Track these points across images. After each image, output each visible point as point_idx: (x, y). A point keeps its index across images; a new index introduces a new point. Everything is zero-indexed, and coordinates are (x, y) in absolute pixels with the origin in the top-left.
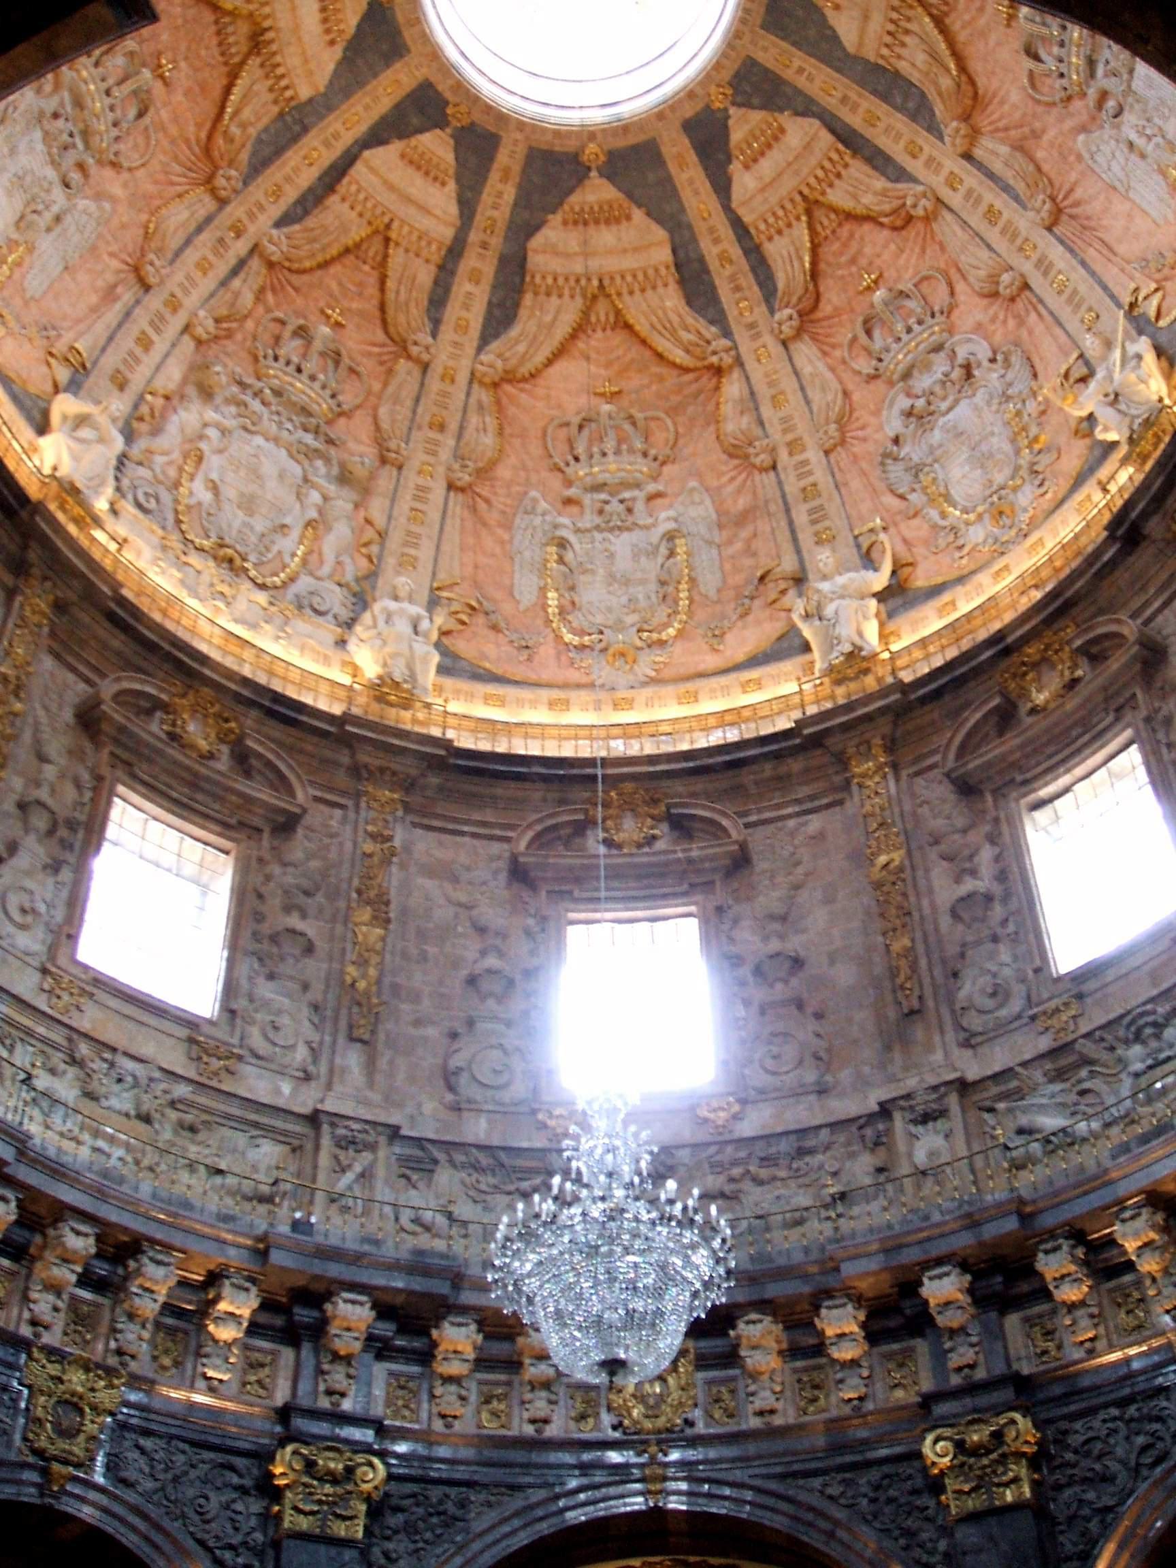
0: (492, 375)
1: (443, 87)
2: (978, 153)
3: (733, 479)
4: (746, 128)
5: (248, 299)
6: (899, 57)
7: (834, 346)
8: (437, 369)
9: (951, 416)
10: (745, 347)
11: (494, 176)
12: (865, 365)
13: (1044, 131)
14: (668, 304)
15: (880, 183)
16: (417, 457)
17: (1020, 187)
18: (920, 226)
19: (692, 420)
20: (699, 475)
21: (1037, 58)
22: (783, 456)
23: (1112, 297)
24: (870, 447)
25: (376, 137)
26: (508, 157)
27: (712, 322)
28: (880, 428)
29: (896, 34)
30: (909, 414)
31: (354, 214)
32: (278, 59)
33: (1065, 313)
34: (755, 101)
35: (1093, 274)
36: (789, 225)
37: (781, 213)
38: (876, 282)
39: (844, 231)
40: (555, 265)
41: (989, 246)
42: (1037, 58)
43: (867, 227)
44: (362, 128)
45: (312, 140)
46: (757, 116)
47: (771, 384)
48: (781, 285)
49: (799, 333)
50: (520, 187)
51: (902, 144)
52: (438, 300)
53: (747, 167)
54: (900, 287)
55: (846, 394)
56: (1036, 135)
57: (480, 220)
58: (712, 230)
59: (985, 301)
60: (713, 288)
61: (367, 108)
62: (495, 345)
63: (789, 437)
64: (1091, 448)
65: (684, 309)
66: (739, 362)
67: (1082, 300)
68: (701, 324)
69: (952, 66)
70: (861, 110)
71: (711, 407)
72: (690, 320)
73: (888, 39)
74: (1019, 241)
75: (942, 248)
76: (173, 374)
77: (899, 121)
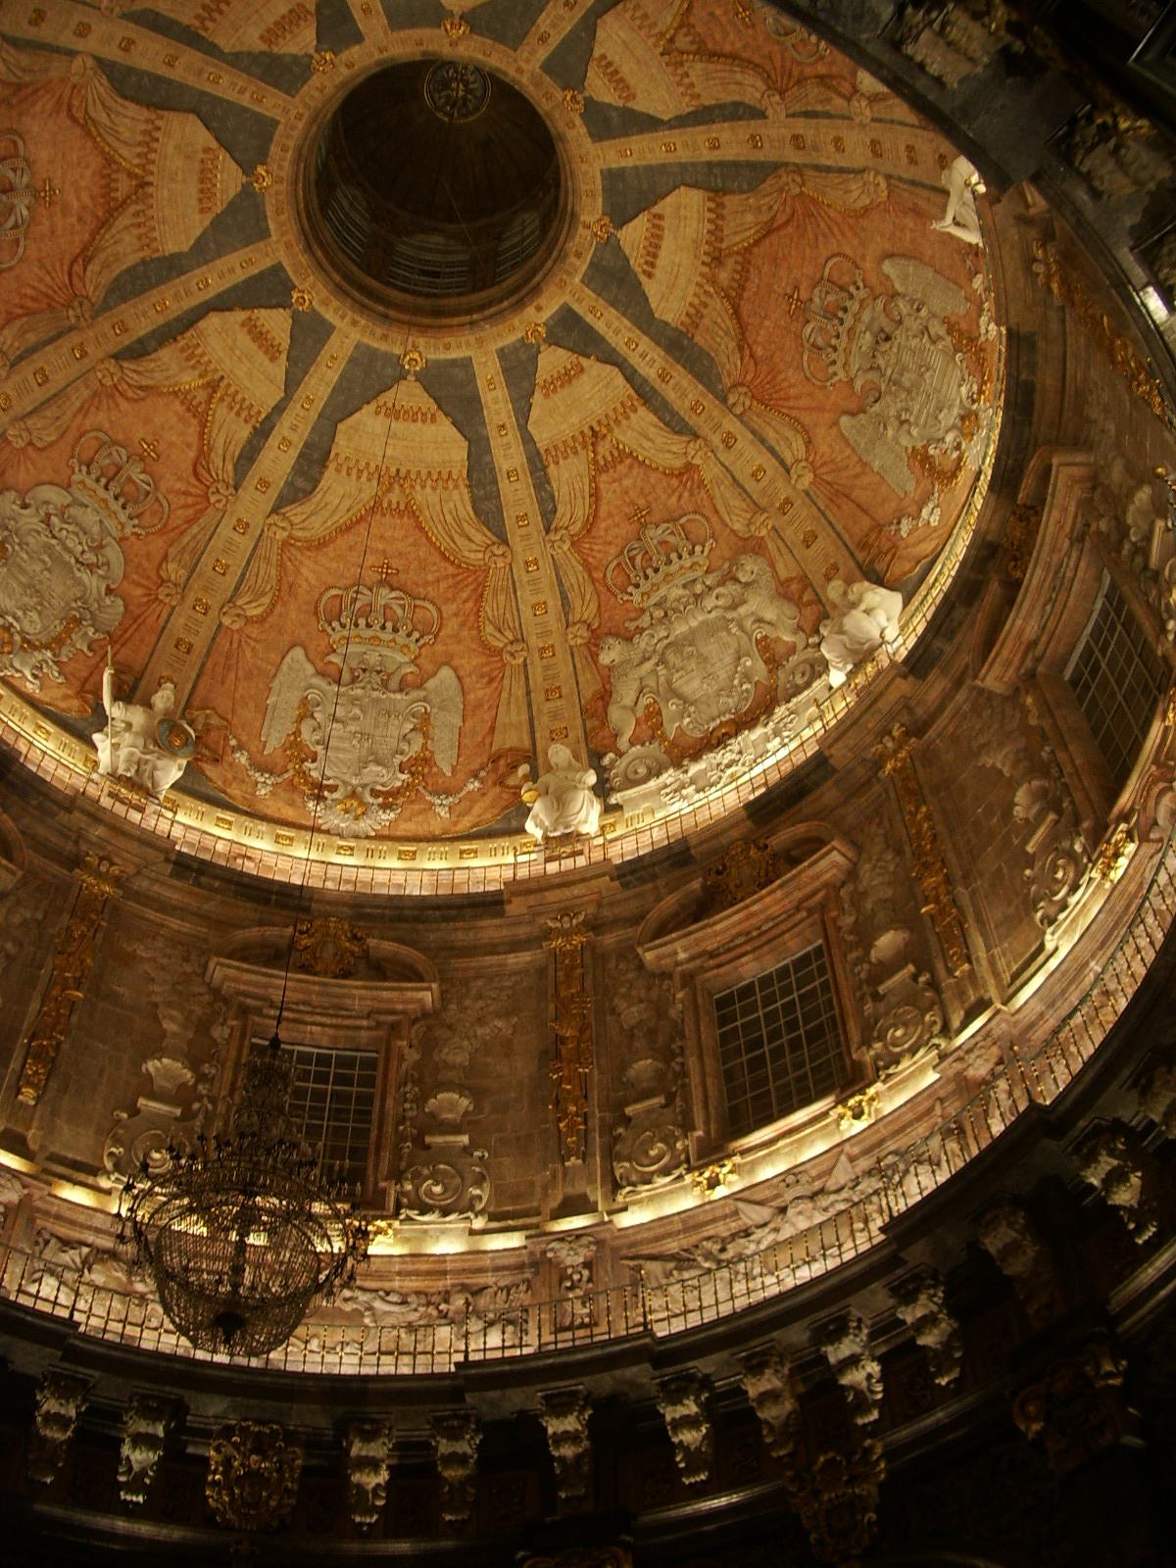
6: (147, 121)
11: (554, 41)
25: (651, 123)
29: (149, 141)
31: (693, 78)
32: (707, 237)
44: (660, 135)
45: (707, 155)
50: (533, 22)
61: (651, 151)
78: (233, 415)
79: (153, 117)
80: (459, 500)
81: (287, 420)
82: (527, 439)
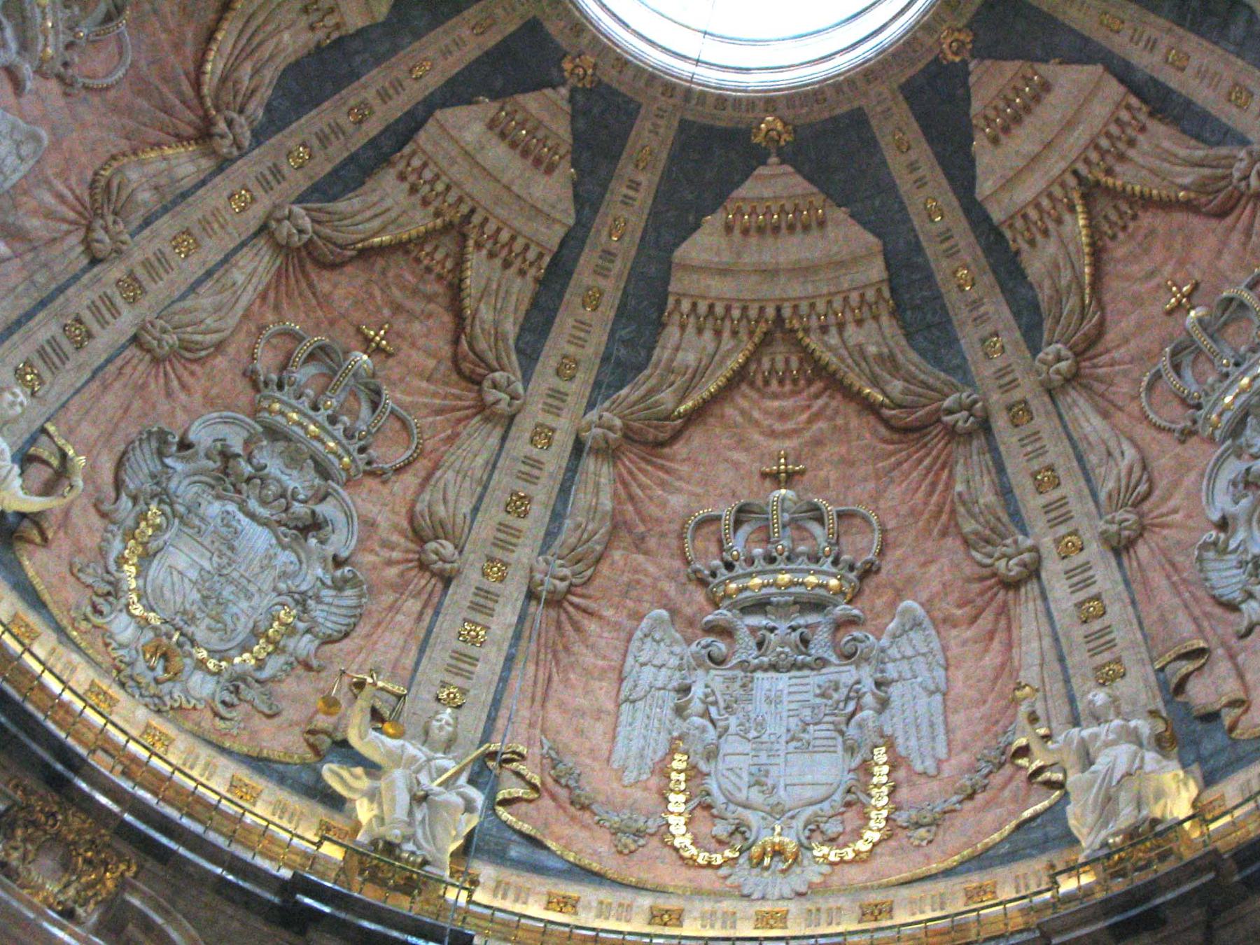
2: (590, 464)
3: (61, 198)
4: (546, 118)
6: (683, 327)
7: (277, 308)
9: (245, 520)
10: (246, 169)
12: (266, 363)
13: (646, 553)
14: (286, 36)
15: (510, 328)
17: (568, 535)
18: (470, 397)
19: (130, 111)
20: (56, 143)
21: (738, 523)
22: (115, 272)
23: (491, 719)
24: (164, 406)
27: (269, 109)
28: (194, 415)
30: (227, 456)
33: (439, 655)
34: (581, 124)
35: (504, 680)
36: (425, 202)
37: (440, 187)
38: (379, 349)
39: (433, 287)
41: (476, 510)
42: (738, 523)
43: (447, 318)
46: (562, 128)
47: (205, 224)
48: (341, 206)
49: (281, 248)
51: (571, 349)
53: (491, 125)
54: (386, 391)
55: (219, 347)
56: (639, 544)
58: (398, 85)
59: (405, 524)
63: (140, 272)
64: (304, 764)
65: (281, 62)
66: (223, 165)
67: (469, 676)
68: (265, 93)
69: (689, 404)
70: (602, 283)
71: (153, 135)
72: (270, 74)
73: (703, 307)
74: (498, 553)
75: (450, 440)
77: (597, 340)
78: (1131, 153)
79: (676, 317)
81: (1145, 61)
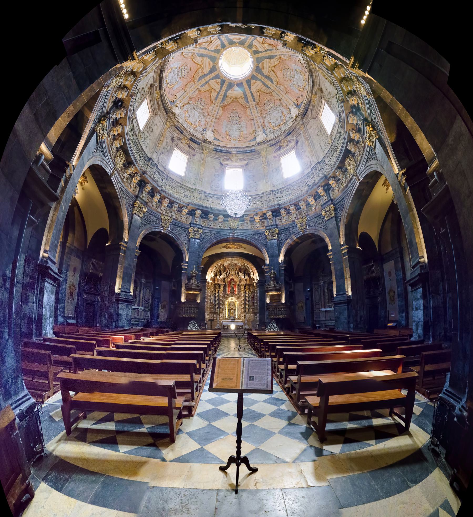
0: (277, 84)
1: (247, 79)
5: (259, 108)
8: (274, 90)
16: (281, 96)
25: (250, 88)
26: (255, 74)
40: (267, 72)
44: (248, 89)
52: (268, 87)
57: (261, 79)
60: (272, 55)
62: (274, 82)
76: (262, 121)
80: (201, 74)
81: (207, 51)
82: (209, 80)
